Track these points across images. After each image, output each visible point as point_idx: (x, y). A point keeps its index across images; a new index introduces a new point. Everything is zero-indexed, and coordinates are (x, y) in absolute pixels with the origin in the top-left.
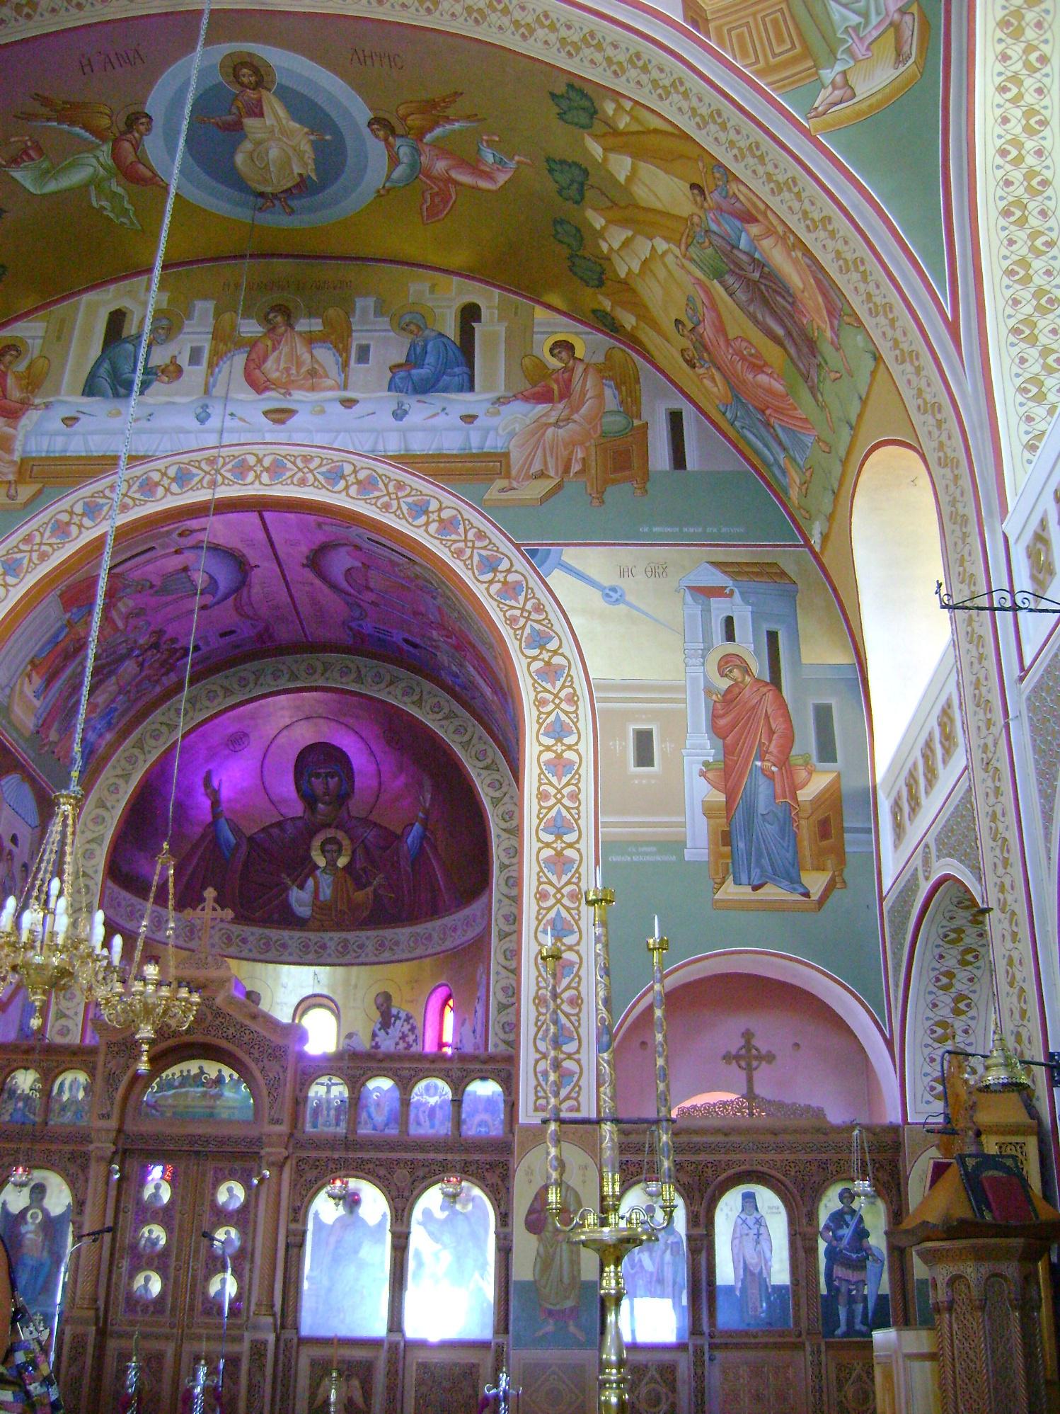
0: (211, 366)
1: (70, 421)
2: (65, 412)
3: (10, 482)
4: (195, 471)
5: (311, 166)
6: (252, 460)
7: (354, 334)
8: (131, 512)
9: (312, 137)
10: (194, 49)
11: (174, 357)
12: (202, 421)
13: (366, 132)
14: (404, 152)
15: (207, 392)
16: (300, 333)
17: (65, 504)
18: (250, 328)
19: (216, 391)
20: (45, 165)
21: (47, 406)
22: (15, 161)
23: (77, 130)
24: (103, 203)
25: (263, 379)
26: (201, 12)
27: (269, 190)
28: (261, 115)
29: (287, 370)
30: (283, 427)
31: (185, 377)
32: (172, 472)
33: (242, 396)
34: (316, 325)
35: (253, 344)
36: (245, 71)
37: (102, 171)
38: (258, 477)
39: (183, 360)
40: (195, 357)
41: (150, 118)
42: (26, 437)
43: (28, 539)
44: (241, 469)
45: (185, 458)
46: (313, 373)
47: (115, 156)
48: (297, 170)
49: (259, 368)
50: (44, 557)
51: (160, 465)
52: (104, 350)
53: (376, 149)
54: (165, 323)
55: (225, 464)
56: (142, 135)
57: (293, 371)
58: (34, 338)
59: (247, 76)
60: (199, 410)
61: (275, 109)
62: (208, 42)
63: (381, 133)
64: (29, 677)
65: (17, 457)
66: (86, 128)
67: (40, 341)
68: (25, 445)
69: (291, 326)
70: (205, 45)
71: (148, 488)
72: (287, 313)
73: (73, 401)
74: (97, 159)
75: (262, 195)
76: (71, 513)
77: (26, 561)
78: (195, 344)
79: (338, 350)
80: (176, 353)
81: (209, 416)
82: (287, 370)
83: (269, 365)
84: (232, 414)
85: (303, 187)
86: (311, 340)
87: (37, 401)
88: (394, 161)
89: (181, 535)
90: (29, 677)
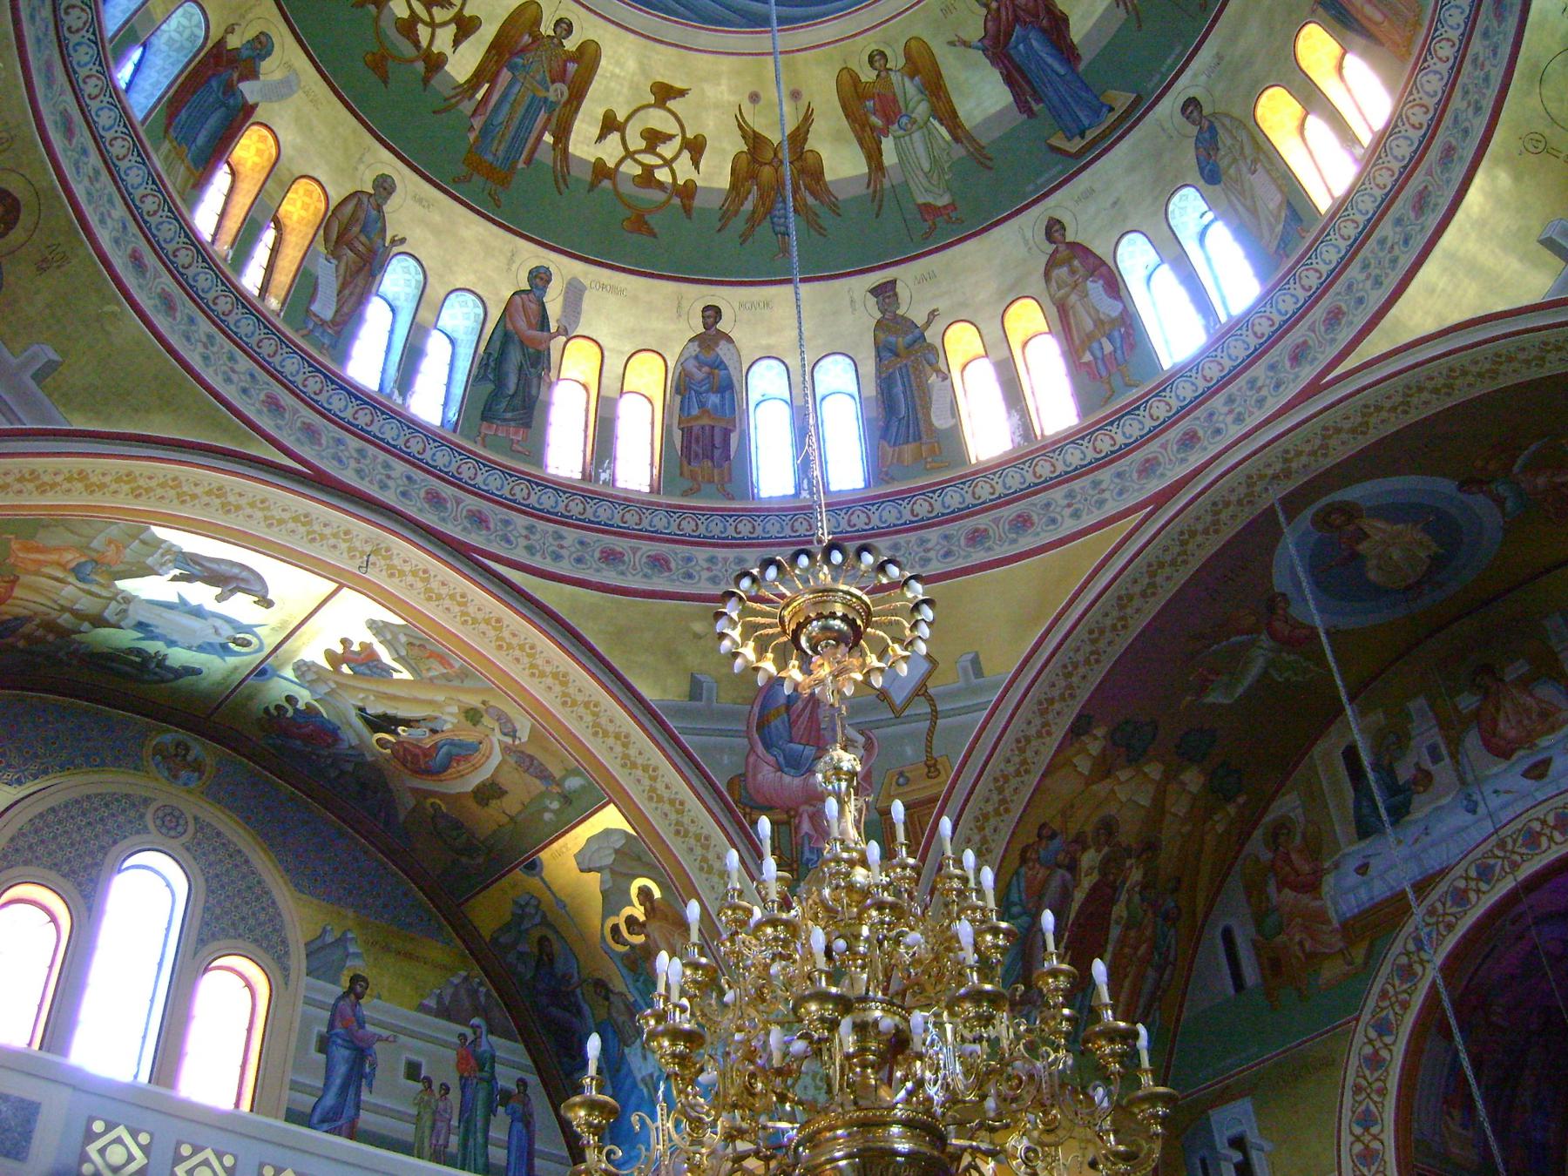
0: (1453, 756)
1: (1363, 869)
2: (1354, 863)
3: (1341, 951)
4: (1492, 861)
5: (1435, 548)
6: (1536, 826)
7: (1560, 656)
8: (1458, 928)
9: (1419, 526)
10: (1282, 533)
11: (1417, 764)
12: (1474, 812)
13: (1461, 496)
14: (1501, 489)
15: (1463, 782)
16: (1512, 682)
17: (1397, 947)
18: (1468, 702)
19: (1470, 778)
20: (1225, 678)
21: (1337, 866)
22: (1202, 690)
23: (1233, 639)
24: (1286, 675)
25: (1502, 743)
26: (1273, 505)
27: (1410, 581)
28: (1367, 536)
29: (1520, 722)
30: (1546, 780)
31: (1437, 779)
32: (1473, 873)
33: (1495, 770)
34: (1520, 668)
35: (1477, 715)
36: (1333, 517)
37: (1270, 654)
38: (1551, 839)
39: (1427, 764)
40: (1436, 757)
41: (1284, 595)
42: (1335, 903)
43: (1384, 995)
44: (1532, 839)
45: (1478, 853)
46: (1544, 715)
47: (1273, 635)
48: (1423, 555)
49: (1494, 735)
50: (1405, 1006)
51: (1459, 871)
52: (1355, 790)
53: (1479, 503)
54: (1392, 738)
55: (1515, 841)
56: (1284, 610)
57: (1526, 722)
58: (1294, 809)
59: (1337, 519)
60: (1465, 802)
61: (1377, 528)
62: (1289, 521)
63: (1474, 489)
64: (1449, 1114)
65: (1335, 923)
66: (1239, 632)
67: (1300, 811)
68: (1336, 912)
69: (1501, 680)
70: (1288, 524)
71: (1460, 897)
72: (1488, 669)
73: (1355, 850)
74: (1261, 647)
75: (1409, 588)
76: (1407, 954)
77: (1392, 1017)
78: (1428, 743)
79: (1555, 679)
80: (1416, 760)
81: (1476, 803)
82: (1520, 722)
83: (1502, 726)
84: (1496, 792)
85: (1437, 563)
86: (1525, 683)
87: (1327, 865)
88: (1499, 501)
89: (1513, 923)
90: (1449, 1114)
